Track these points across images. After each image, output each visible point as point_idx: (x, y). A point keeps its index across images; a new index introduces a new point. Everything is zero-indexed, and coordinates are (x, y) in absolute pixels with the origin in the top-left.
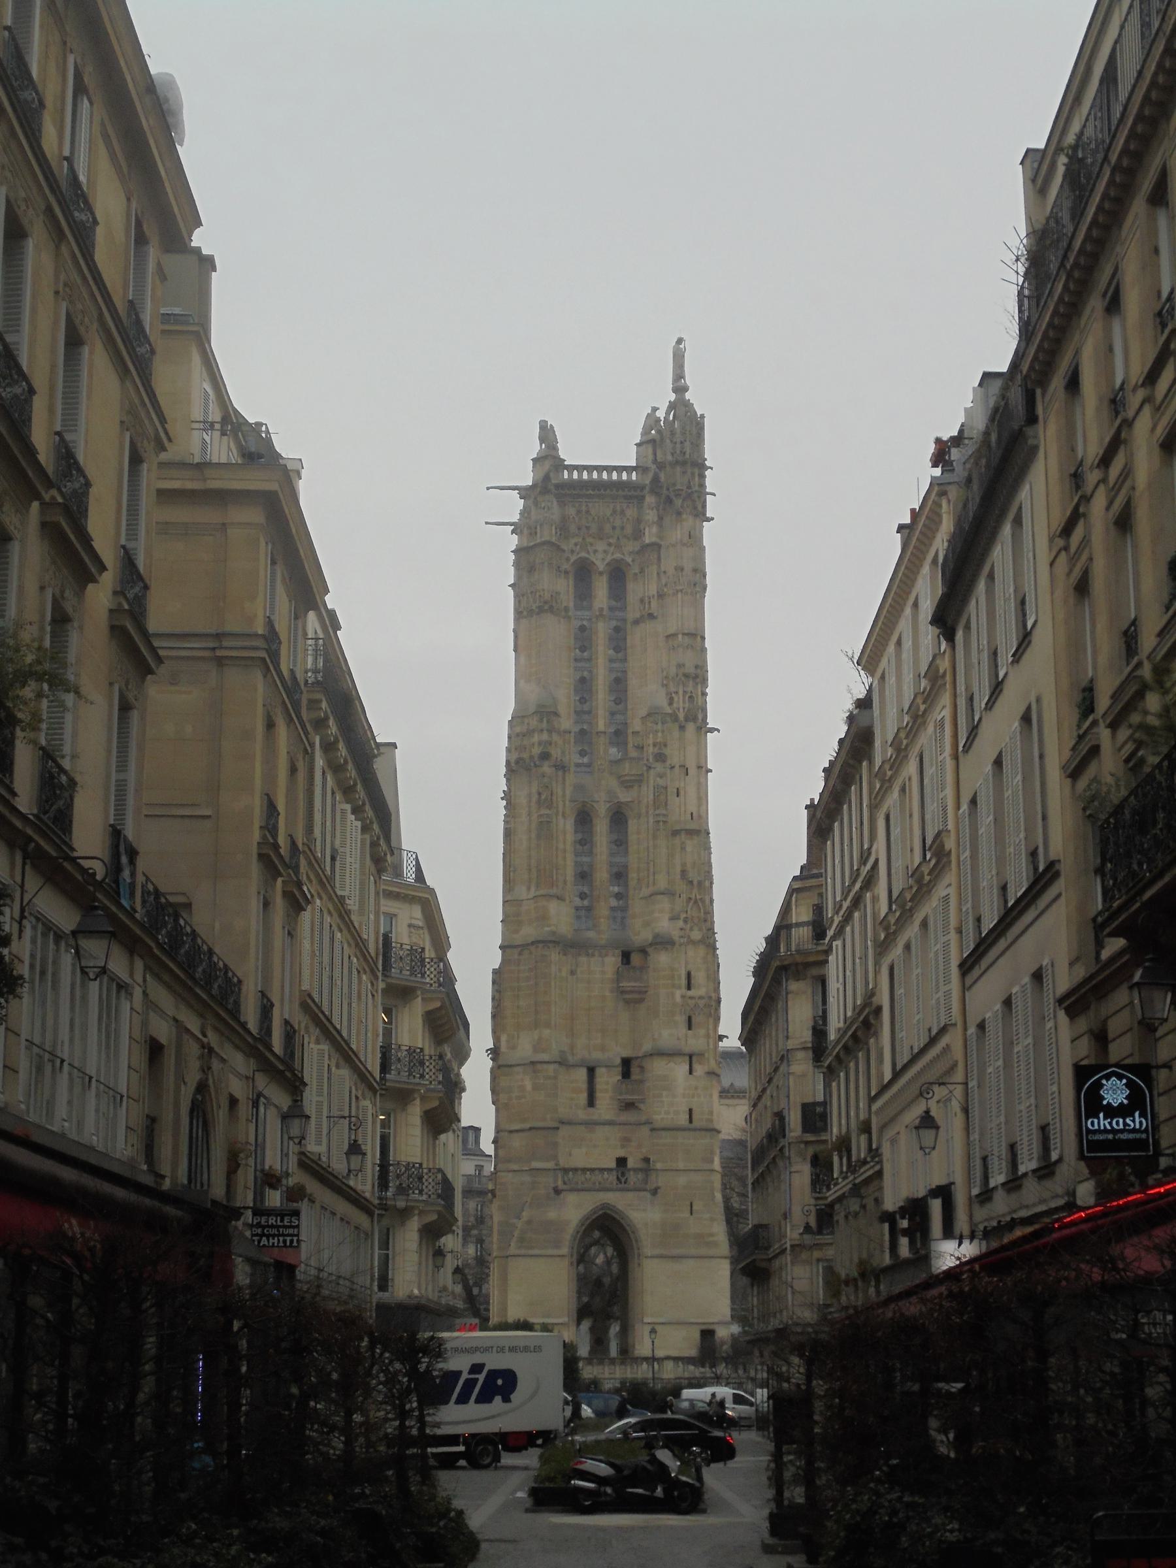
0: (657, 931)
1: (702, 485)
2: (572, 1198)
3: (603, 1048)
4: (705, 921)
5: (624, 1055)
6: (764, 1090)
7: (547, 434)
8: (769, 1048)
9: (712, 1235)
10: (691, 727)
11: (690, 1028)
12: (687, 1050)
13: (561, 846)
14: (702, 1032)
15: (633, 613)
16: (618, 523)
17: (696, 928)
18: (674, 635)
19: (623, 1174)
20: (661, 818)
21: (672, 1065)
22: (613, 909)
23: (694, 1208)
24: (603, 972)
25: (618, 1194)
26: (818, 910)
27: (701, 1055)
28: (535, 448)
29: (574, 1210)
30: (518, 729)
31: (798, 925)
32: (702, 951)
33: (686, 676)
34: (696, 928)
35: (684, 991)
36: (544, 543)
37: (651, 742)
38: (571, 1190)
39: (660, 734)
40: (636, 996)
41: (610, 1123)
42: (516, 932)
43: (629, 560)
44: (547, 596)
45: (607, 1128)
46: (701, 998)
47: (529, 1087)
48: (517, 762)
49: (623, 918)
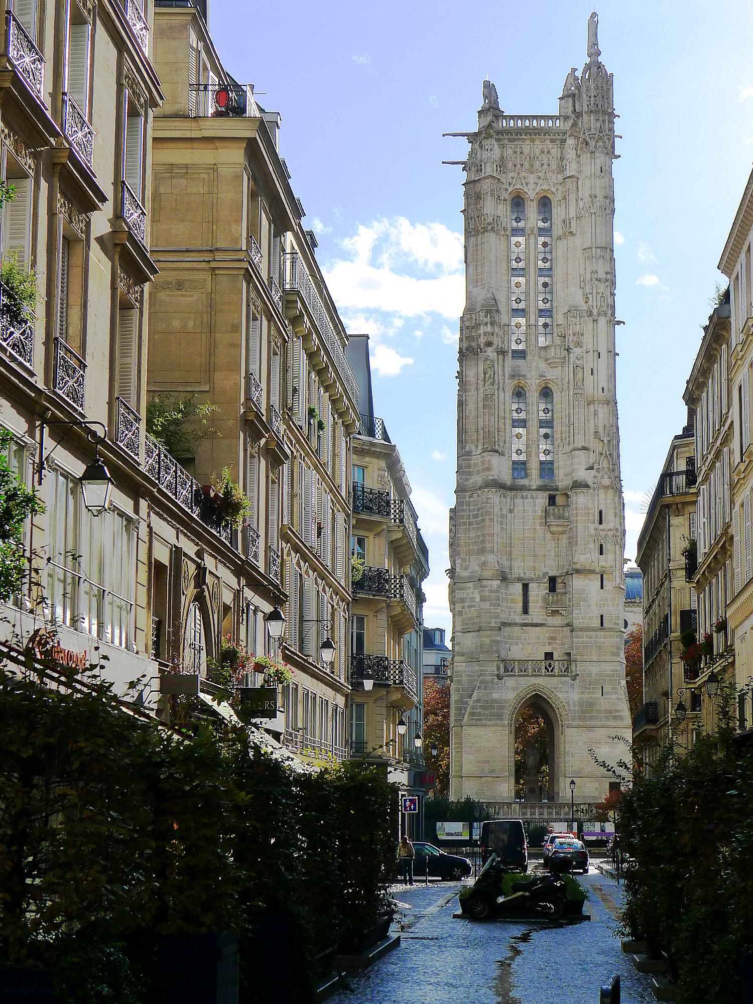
0: (575, 479)
1: (612, 130)
2: (510, 682)
5: (551, 574)
6: (653, 601)
7: (489, 90)
8: (656, 569)
9: (619, 711)
10: (602, 321)
11: (601, 554)
12: (598, 570)
13: (501, 414)
15: (557, 230)
16: (545, 162)
19: (550, 666)
21: (587, 582)
22: (542, 463)
24: (535, 511)
25: (546, 678)
26: (691, 461)
28: (480, 103)
29: (511, 692)
30: (467, 324)
31: (678, 473)
32: (611, 492)
33: (599, 280)
34: (606, 476)
35: (597, 524)
36: (487, 177)
39: (578, 326)
40: (560, 529)
43: (554, 190)
44: (490, 220)
47: (478, 599)
48: (467, 349)
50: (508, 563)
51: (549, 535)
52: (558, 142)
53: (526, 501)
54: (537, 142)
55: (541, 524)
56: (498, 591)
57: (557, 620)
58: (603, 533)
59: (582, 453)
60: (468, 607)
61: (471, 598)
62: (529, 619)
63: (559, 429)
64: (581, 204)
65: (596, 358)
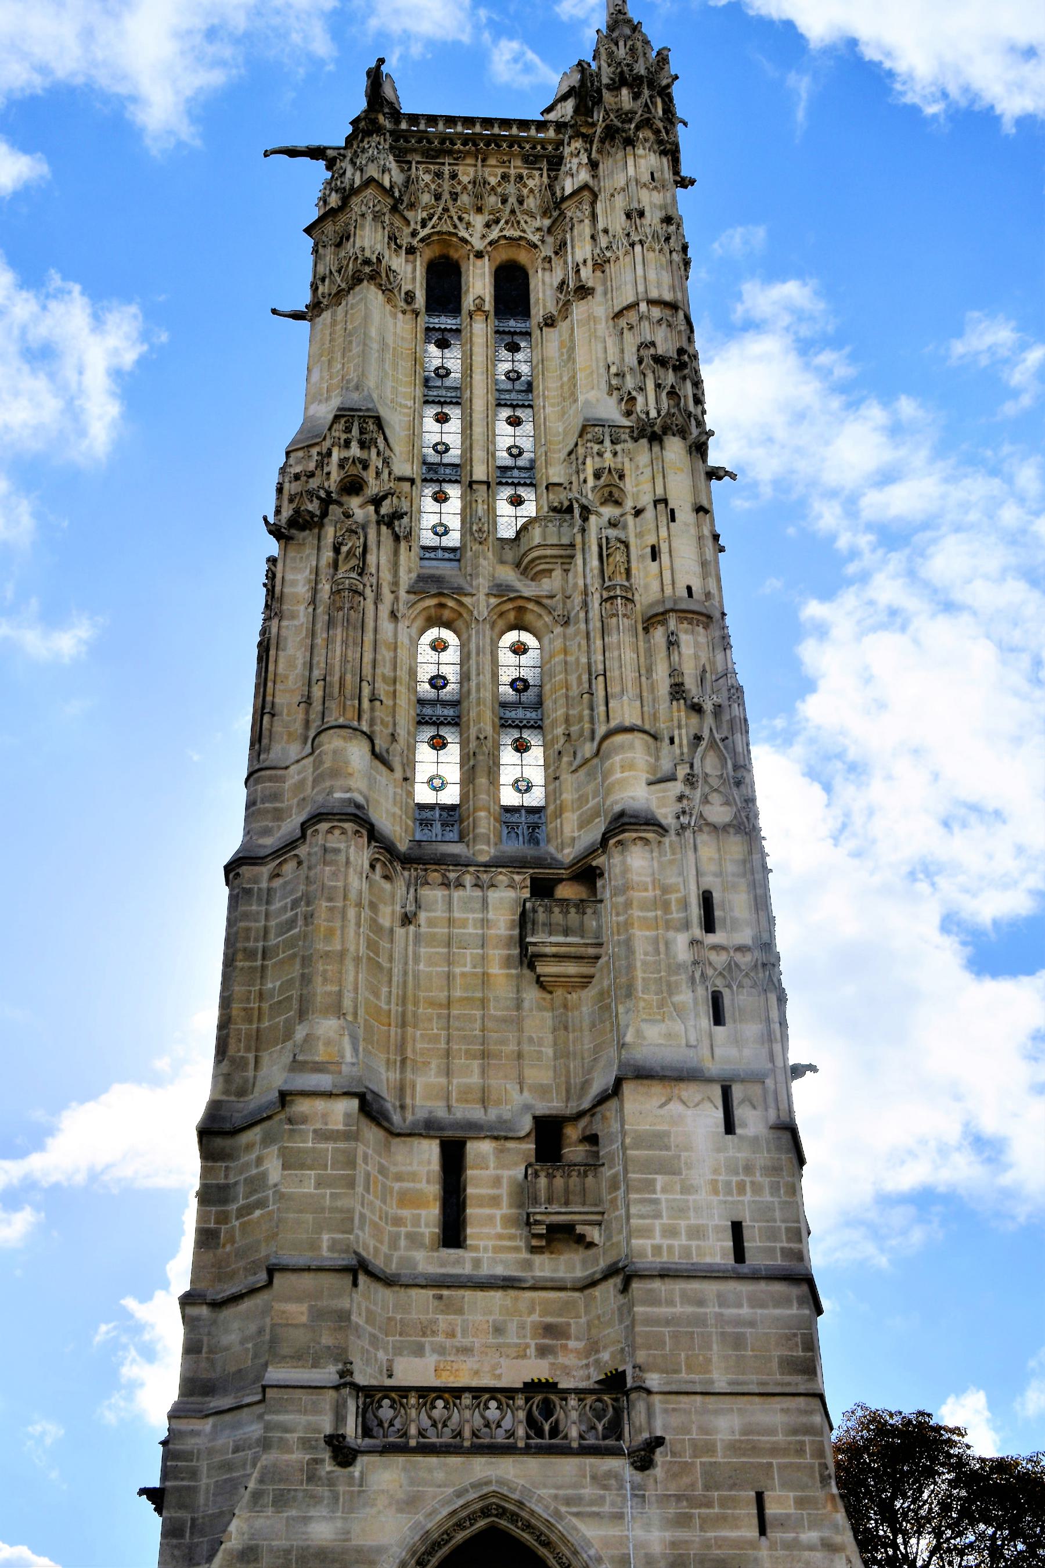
0: (617, 808)
2: (385, 1475)
4: (738, 783)
5: (543, 1108)
11: (718, 1019)
12: (712, 1068)
14: (752, 1029)
17: (715, 798)
18: (634, 306)
20: (618, 592)
21: (675, 1107)
23: (771, 1510)
24: (485, 923)
25: (533, 1464)
27: (757, 1078)
30: (298, 469)
32: (735, 846)
33: (660, 361)
34: (715, 798)
35: (697, 932)
38: (388, 1450)
40: (571, 969)
41: (508, 1284)
42: (266, 832)
43: (535, 238)
45: (497, 1296)
46: (741, 949)
49: (534, 827)
50: (394, 1076)
51: (532, 995)
52: (544, 165)
53: (457, 894)
54: (492, 161)
55: (508, 962)
56: (349, 1136)
57: (568, 1265)
58: (719, 959)
59: (637, 740)
61: (250, 1181)
62: (458, 1262)
64: (604, 241)
65: (663, 520)
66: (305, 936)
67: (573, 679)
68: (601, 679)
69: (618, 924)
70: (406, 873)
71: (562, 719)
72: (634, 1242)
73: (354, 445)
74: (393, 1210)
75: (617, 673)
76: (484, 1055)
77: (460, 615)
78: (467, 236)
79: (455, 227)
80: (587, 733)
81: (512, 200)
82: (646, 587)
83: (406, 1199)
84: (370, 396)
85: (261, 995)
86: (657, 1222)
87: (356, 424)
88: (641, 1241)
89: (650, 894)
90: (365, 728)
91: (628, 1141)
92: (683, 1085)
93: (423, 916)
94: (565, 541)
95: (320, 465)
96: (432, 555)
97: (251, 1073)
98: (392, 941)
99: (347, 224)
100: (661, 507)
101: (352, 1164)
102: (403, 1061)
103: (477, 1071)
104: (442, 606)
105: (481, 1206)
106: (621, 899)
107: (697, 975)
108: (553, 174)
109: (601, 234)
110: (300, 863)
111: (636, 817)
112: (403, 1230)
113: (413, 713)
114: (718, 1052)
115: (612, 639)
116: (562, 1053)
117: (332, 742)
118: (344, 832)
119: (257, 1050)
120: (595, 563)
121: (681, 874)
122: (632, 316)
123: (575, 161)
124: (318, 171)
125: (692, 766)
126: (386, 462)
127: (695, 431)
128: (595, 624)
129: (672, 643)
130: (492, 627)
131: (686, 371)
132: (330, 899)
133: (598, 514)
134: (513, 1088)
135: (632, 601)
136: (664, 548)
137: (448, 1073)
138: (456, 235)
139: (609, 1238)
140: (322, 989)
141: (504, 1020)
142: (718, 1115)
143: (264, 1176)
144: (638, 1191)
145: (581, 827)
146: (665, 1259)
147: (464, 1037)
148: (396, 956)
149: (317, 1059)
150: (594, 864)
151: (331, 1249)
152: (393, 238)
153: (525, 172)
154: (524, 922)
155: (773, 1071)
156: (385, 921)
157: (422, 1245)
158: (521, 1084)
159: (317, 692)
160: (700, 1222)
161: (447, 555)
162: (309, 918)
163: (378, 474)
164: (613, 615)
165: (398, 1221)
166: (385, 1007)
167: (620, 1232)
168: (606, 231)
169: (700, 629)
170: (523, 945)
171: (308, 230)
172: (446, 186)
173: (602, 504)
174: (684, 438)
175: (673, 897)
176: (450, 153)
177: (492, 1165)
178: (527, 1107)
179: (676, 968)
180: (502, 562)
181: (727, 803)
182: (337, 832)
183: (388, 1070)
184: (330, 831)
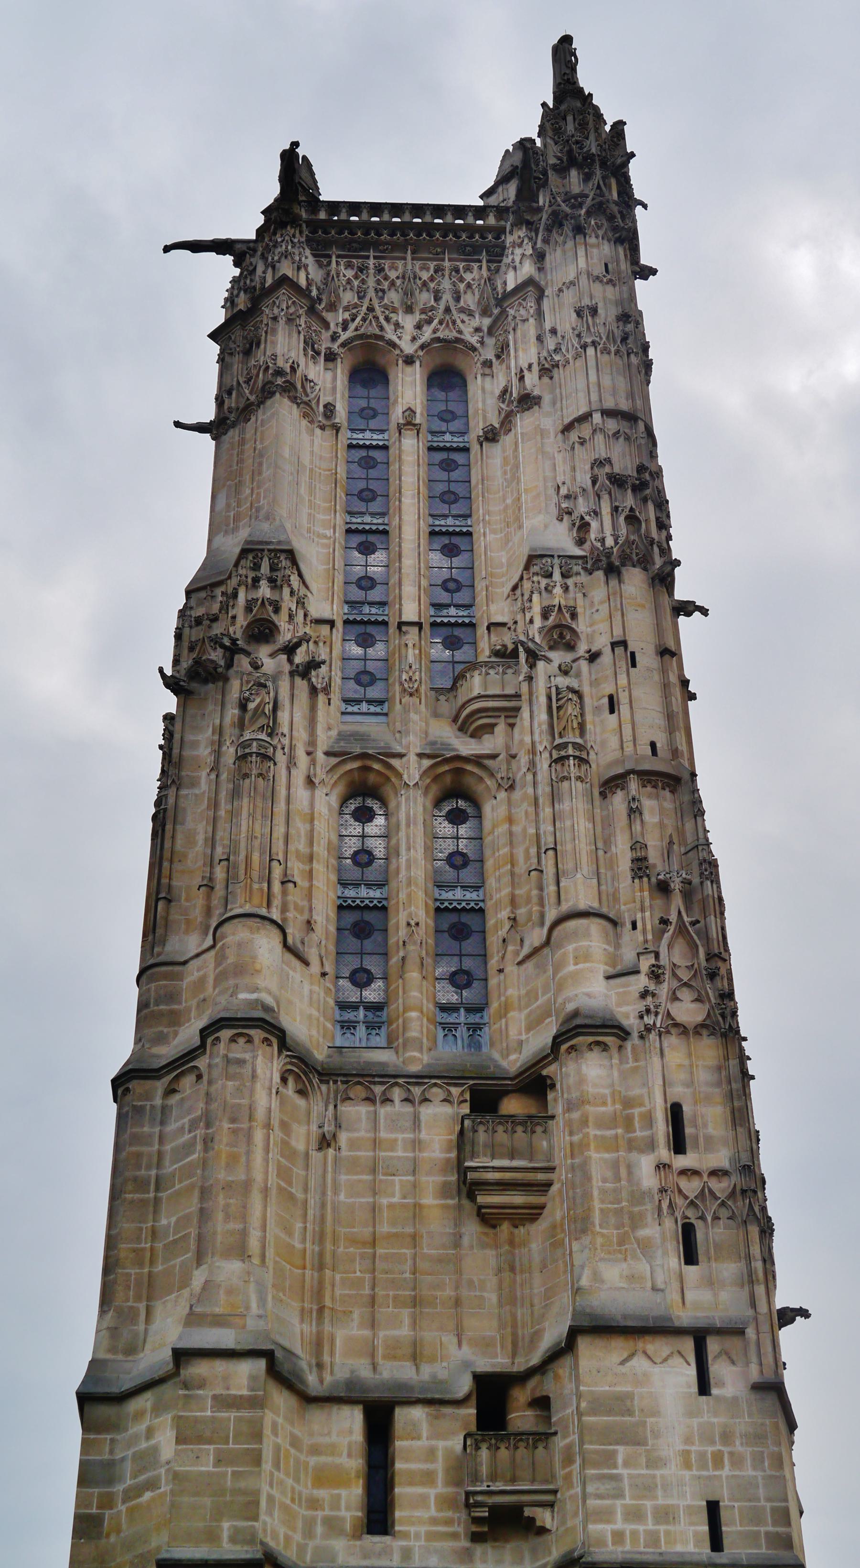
0: (570, 1007)
3: (416, 1357)
4: (712, 975)
5: (485, 1365)
11: (690, 1257)
12: (684, 1317)
13: (299, 845)
14: (729, 1269)
20: (570, 751)
21: (639, 1364)
24: (416, 1144)
30: (199, 612)
32: (708, 1050)
33: (618, 481)
34: (686, 995)
35: (664, 1153)
37: (537, 609)
40: (518, 1199)
42: (161, 1039)
43: (474, 340)
49: (475, 1028)
51: (472, 1229)
52: (484, 257)
53: (384, 1111)
55: (444, 1191)
56: (256, 1402)
58: (691, 1187)
59: (595, 926)
60: (128, 1495)
61: (139, 1457)
63: (506, 891)
65: (623, 664)
66: (204, 1164)
67: (520, 853)
68: (551, 853)
69: (571, 1144)
70: (324, 1087)
71: (507, 901)
72: (591, 1527)
73: (264, 583)
74: (307, 1489)
75: (569, 847)
76: (415, 1302)
77: (388, 779)
78: (394, 338)
79: (381, 328)
80: (535, 917)
81: (447, 297)
82: (603, 743)
83: (322, 1478)
84: (282, 526)
85: (154, 1234)
86: (619, 1503)
87: (266, 559)
88: (600, 1527)
89: (609, 1109)
90: (275, 915)
91: (583, 1405)
92: (648, 1338)
93: (343, 1138)
94: (509, 691)
95: (225, 607)
96: (355, 709)
97: (142, 1327)
98: (307, 1167)
99: (257, 328)
100: (619, 650)
101: (257, 1436)
102: (321, 1310)
103: (407, 1321)
104: (366, 769)
105: (411, 1484)
106: (575, 1115)
107: (665, 1205)
108: (493, 266)
109: (548, 335)
110: (199, 1077)
111: (591, 1017)
112: (320, 1513)
113: (332, 895)
114: (690, 1296)
115: (565, 806)
116: (509, 1298)
117: (236, 933)
118: (250, 1040)
119: (149, 1299)
120: (544, 717)
121: (645, 1084)
122: (585, 430)
123: (518, 251)
124: (224, 269)
125: (657, 955)
126: (301, 603)
127: (658, 562)
128: (543, 789)
129: (634, 812)
130: (426, 793)
131: (648, 492)
132: (233, 1120)
133: (548, 660)
134: (449, 1340)
135: (587, 762)
136: (623, 698)
137: (373, 1324)
138: (381, 338)
139: (563, 1522)
140: (221, 1227)
141: (440, 1260)
142: (692, 1372)
143: (155, 1451)
144: (596, 1465)
145: (529, 1029)
146: (628, 1547)
147: (393, 1281)
148: (312, 1184)
149: (217, 1310)
150: (544, 1072)
151: (233, 1540)
152: (310, 344)
153: (461, 265)
154: (462, 1142)
155: (756, 1319)
156: (299, 1145)
157: (341, 1533)
158: (459, 1337)
159: (220, 873)
160: (670, 1502)
161: (373, 709)
162: (208, 1142)
163: (291, 617)
164: (564, 778)
165: (314, 1504)
166: (298, 1245)
167: (576, 1514)
168: (554, 331)
169: (667, 793)
170: (463, 1171)
171: (214, 336)
172: (371, 282)
173: (551, 648)
174: (645, 569)
175: (636, 1111)
176: (376, 245)
177: (425, 1434)
178: (466, 1364)
179: (638, 1197)
180: (436, 715)
181: (698, 1000)
182: (242, 1040)
183: (302, 1321)
184: (233, 1040)
